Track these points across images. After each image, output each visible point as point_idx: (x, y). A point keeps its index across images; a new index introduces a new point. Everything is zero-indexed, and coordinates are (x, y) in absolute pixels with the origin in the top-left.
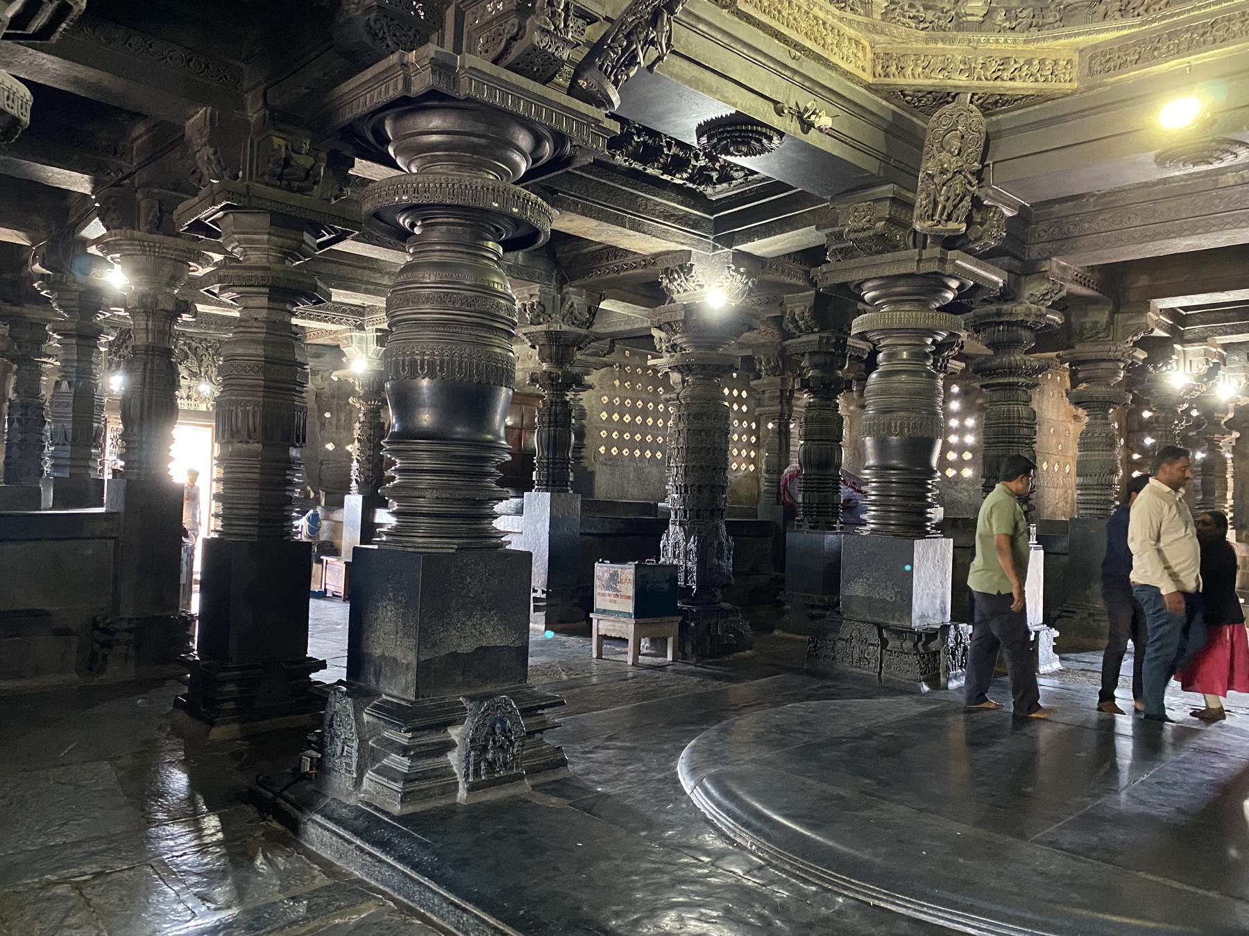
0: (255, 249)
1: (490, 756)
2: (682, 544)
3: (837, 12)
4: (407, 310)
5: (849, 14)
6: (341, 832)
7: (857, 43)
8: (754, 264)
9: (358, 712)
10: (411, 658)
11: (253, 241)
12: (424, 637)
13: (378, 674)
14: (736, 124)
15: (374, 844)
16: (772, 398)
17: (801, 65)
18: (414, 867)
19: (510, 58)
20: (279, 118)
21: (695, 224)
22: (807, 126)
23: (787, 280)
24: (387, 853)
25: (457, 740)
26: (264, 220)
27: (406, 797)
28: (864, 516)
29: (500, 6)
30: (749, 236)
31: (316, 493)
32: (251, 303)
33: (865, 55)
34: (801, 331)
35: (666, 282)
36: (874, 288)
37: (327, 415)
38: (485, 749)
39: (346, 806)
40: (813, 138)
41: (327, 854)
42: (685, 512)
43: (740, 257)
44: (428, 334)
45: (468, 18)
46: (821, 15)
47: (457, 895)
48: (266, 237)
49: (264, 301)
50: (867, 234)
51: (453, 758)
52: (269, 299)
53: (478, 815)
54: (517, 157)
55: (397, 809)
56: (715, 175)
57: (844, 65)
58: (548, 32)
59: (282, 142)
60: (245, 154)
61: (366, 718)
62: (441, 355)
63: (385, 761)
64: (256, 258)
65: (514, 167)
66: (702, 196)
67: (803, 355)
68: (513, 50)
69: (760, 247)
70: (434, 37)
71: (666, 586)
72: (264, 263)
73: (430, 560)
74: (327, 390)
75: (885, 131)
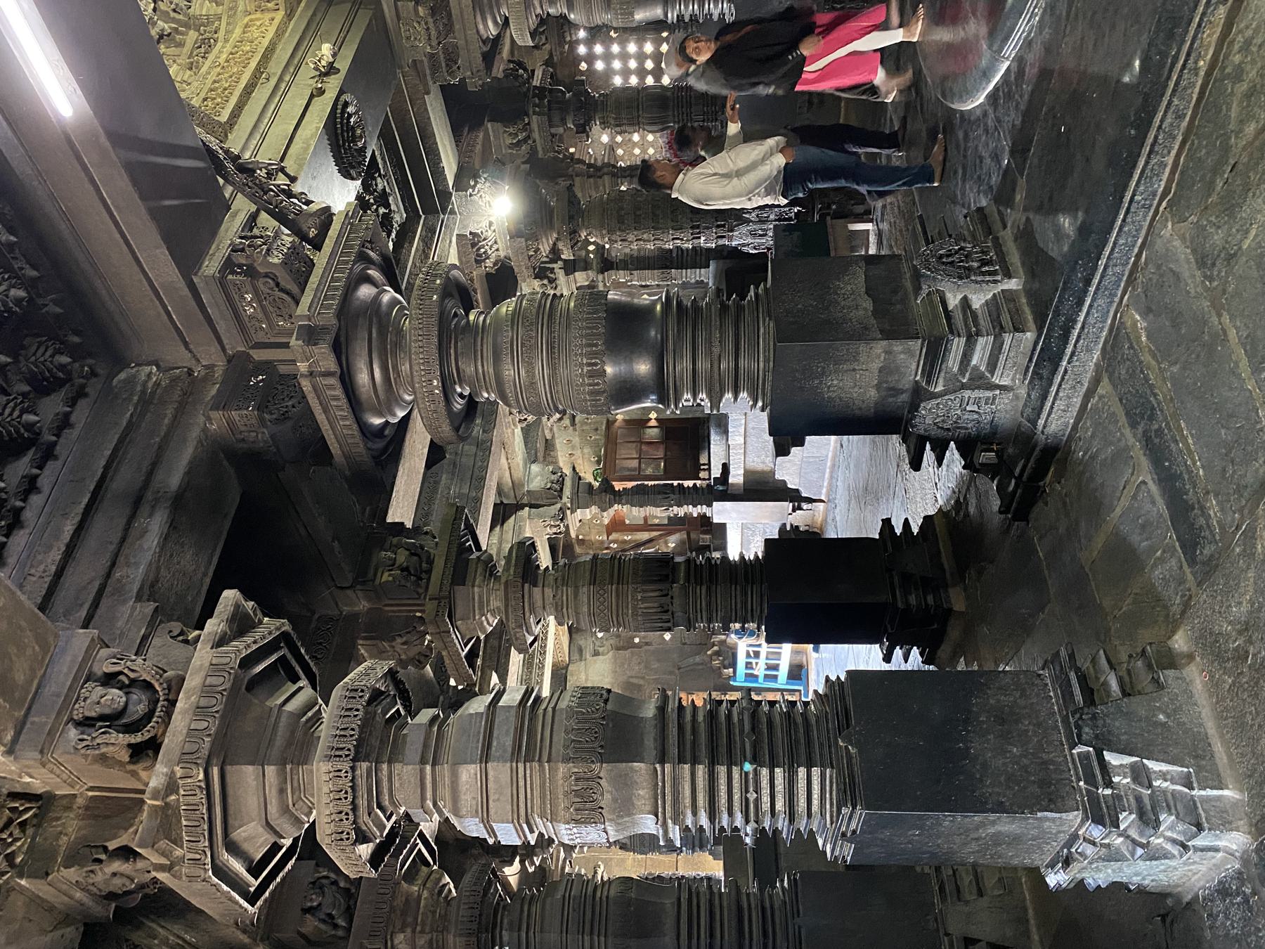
0: (488, 601)
1: (975, 264)
2: (751, 227)
3: (219, 44)
4: (540, 385)
5: (221, 34)
6: (1054, 389)
7: (247, 26)
8: (466, 175)
9: (934, 396)
10: (880, 347)
11: (481, 602)
12: (861, 335)
13: (895, 391)
14: (336, 134)
15: (1066, 342)
16: (597, 188)
17: (274, 74)
18: (1088, 282)
19: (295, 289)
20: (363, 578)
21: (430, 231)
22: (331, 70)
23: (479, 148)
24: (1075, 321)
25: (960, 297)
26: (459, 590)
27: (1018, 328)
28: (715, 18)
29: (248, 297)
30: (439, 173)
31: (714, 645)
32: (539, 603)
33: (258, 19)
34: (529, 137)
35: (489, 263)
36: (486, 26)
37: (637, 640)
38: (969, 269)
39: (1029, 395)
40: (344, 65)
41: (1077, 401)
42: (718, 226)
43: (460, 184)
44: (563, 372)
45: (261, 337)
46: (224, 56)
47: (1117, 214)
48: (476, 589)
49: (537, 591)
50: (431, 25)
51: (978, 300)
52: (535, 586)
53: (1031, 274)
54: (386, 298)
55: (1030, 335)
56: (382, 210)
57: (270, 35)
58: (268, 250)
59: (386, 574)
60: (400, 611)
61: (940, 388)
62: (581, 346)
63: (983, 368)
64: (496, 602)
65: (395, 302)
66: (402, 226)
67: (553, 136)
68: (288, 287)
69: (449, 166)
70: (283, 369)
71: (796, 234)
72: (501, 593)
73: (782, 336)
74: (612, 642)
75: (330, 5)
